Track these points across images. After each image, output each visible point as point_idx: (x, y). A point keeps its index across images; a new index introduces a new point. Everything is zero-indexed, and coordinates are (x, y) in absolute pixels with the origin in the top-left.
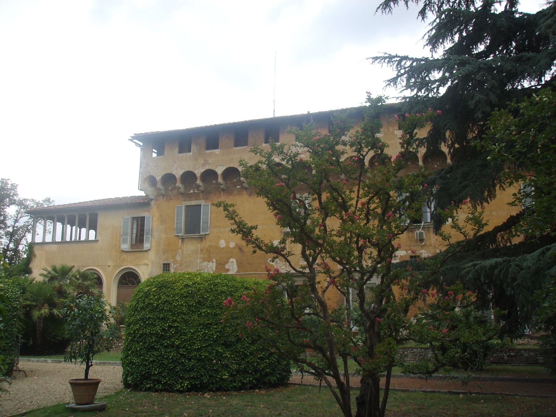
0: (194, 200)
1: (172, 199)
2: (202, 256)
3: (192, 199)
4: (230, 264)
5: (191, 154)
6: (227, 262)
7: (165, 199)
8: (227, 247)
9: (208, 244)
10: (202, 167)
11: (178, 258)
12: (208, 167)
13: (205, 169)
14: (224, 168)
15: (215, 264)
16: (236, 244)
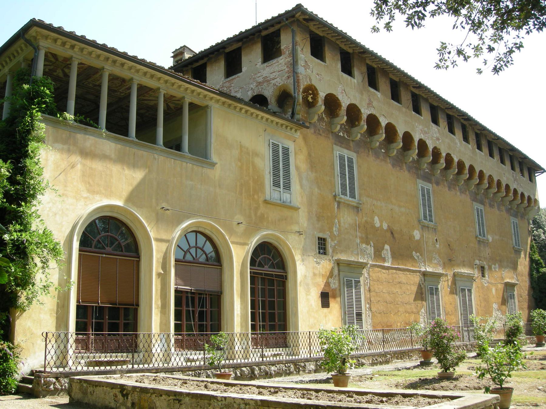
1: (320, 135)
3: (343, 146)
9: (365, 219)
13: (370, 113)
15: (373, 248)
16: (388, 226)
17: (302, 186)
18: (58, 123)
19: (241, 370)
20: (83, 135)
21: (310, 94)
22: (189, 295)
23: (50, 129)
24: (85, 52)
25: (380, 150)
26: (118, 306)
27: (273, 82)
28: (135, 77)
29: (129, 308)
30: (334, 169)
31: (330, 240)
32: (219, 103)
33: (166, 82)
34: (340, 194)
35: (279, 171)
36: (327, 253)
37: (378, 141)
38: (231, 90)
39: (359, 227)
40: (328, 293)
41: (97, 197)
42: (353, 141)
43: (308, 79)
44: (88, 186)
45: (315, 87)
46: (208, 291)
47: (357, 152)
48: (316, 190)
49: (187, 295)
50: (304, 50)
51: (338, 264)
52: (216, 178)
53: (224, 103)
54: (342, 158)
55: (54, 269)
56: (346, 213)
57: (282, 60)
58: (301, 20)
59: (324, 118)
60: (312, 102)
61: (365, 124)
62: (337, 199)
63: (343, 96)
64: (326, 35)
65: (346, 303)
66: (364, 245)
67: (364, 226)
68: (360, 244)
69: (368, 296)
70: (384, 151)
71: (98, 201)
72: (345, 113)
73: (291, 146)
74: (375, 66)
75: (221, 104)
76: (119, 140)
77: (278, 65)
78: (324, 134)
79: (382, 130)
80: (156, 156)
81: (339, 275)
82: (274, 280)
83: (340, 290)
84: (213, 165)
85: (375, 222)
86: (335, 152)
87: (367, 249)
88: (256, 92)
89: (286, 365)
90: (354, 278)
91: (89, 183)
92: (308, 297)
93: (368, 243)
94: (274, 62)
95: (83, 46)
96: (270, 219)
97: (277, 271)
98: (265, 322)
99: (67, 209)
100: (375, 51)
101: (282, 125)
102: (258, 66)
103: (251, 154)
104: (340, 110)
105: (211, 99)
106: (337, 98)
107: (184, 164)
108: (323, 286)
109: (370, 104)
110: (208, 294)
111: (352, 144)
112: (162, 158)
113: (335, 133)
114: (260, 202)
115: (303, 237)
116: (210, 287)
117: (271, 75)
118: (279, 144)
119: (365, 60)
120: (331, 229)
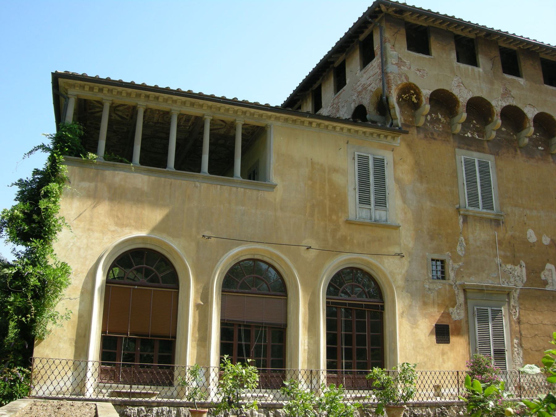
0: (475, 151)
1: (435, 139)
2: (502, 253)
4: (546, 272)
5: (481, 70)
6: (543, 269)
7: (422, 135)
8: (539, 241)
9: (510, 233)
10: (502, 97)
11: (460, 250)
12: (510, 102)
13: (508, 104)
14: (536, 112)
15: (524, 270)
16: (552, 240)
17: (404, 200)
18: (82, 163)
19: (276, 412)
20: (112, 171)
21: (413, 94)
22: (242, 328)
23: (76, 169)
24: (115, 93)
25: (535, 148)
26: (150, 338)
27: (369, 88)
28: (173, 108)
29: (154, 340)
30: (457, 177)
31: (451, 261)
32: (281, 121)
33: (211, 107)
34: (467, 205)
35: (368, 185)
36: (447, 277)
37: (526, 137)
38: (339, 106)
39: (500, 243)
40: (447, 326)
41: (127, 230)
42: (488, 141)
43: (403, 77)
44: (116, 219)
45: (415, 85)
46: (265, 324)
47: (496, 154)
48: (428, 204)
49: (239, 328)
50: (397, 46)
51: (464, 291)
52: (278, 200)
53: (286, 120)
54: (469, 164)
55: (75, 299)
56: (478, 228)
57: (375, 63)
58: (392, 13)
59: (440, 120)
60: (418, 103)
61: (499, 118)
62: (461, 212)
63: (460, 90)
64: (431, 25)
65: (477, 338)
66: (509, 266)
67: (510, 242)
68: (503, 265)
69: (517, 329)
70: (543, 149)
71: (127, 233)
72: (465, 109)
73: (388, 157)
74: (515, 48)
75: (283, 121)
76: (152, 171)
77: (373, 68)
78: (440, 138)
79: (529, 122)
80: (198, 184)
81: (466, 303)
82: (365, 310)
83: (467, 322)
84: (273, 187)
85: (528, 236)
86: (457, 157)
87: (515, 270)
88: (357, 103)
89: (374, 410)
90: (491, 307)
91: (117, 216)
92: (414, 330)
93: (515, 262)
94: (369, 67)
95: (111, 87)
96: (355, 241)
97: (365, 301)
98: (351, 359)
99: (92, 243)
100: (503, 30)
101: (372, 134)
102: (357, 74)
103: (327, 171)
104: (458, 107)
105: (270, 117)
106: (452, 93)
107: (234, 189)
108: (438, 318)
109: (506, 94)
110: (268, 327)
111: (486, 145)
112: (204, 186)
113: (458, 134)
114: (341, 223)
115: (405, 261)
116: (277, 320)
117: (368, 81)
118: (369, 155)
119: (497, 43)
120: (452, 249)
